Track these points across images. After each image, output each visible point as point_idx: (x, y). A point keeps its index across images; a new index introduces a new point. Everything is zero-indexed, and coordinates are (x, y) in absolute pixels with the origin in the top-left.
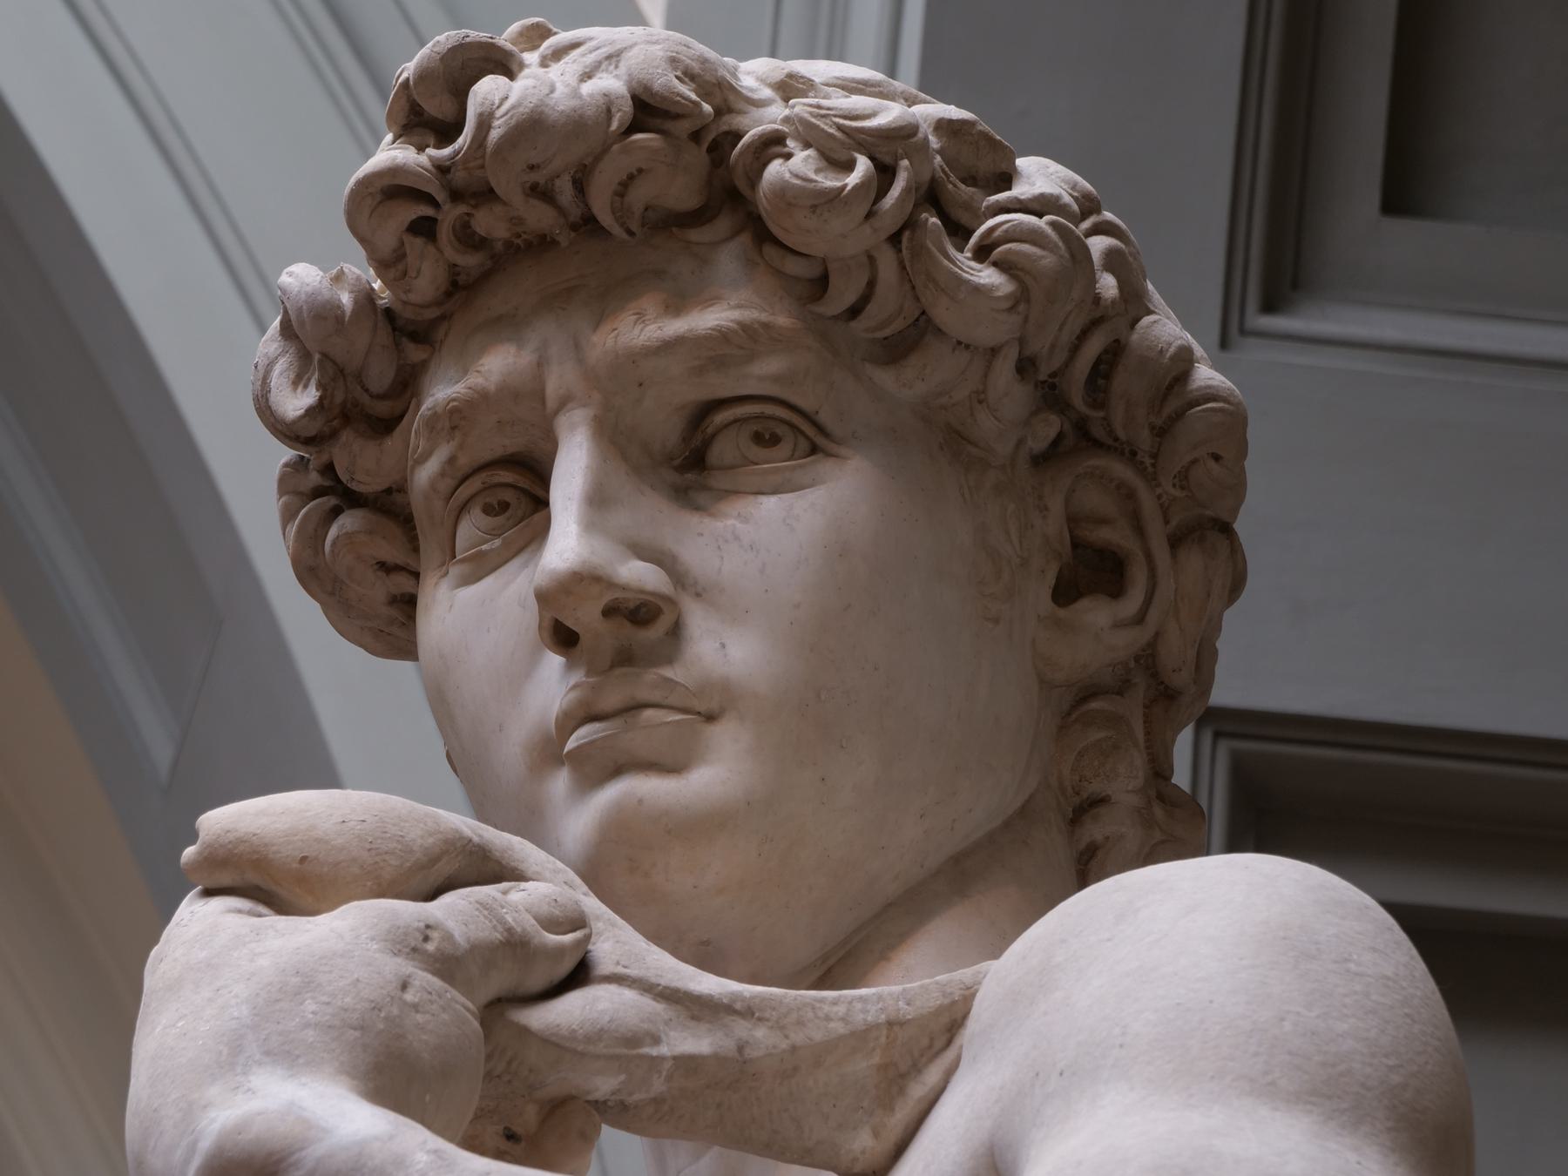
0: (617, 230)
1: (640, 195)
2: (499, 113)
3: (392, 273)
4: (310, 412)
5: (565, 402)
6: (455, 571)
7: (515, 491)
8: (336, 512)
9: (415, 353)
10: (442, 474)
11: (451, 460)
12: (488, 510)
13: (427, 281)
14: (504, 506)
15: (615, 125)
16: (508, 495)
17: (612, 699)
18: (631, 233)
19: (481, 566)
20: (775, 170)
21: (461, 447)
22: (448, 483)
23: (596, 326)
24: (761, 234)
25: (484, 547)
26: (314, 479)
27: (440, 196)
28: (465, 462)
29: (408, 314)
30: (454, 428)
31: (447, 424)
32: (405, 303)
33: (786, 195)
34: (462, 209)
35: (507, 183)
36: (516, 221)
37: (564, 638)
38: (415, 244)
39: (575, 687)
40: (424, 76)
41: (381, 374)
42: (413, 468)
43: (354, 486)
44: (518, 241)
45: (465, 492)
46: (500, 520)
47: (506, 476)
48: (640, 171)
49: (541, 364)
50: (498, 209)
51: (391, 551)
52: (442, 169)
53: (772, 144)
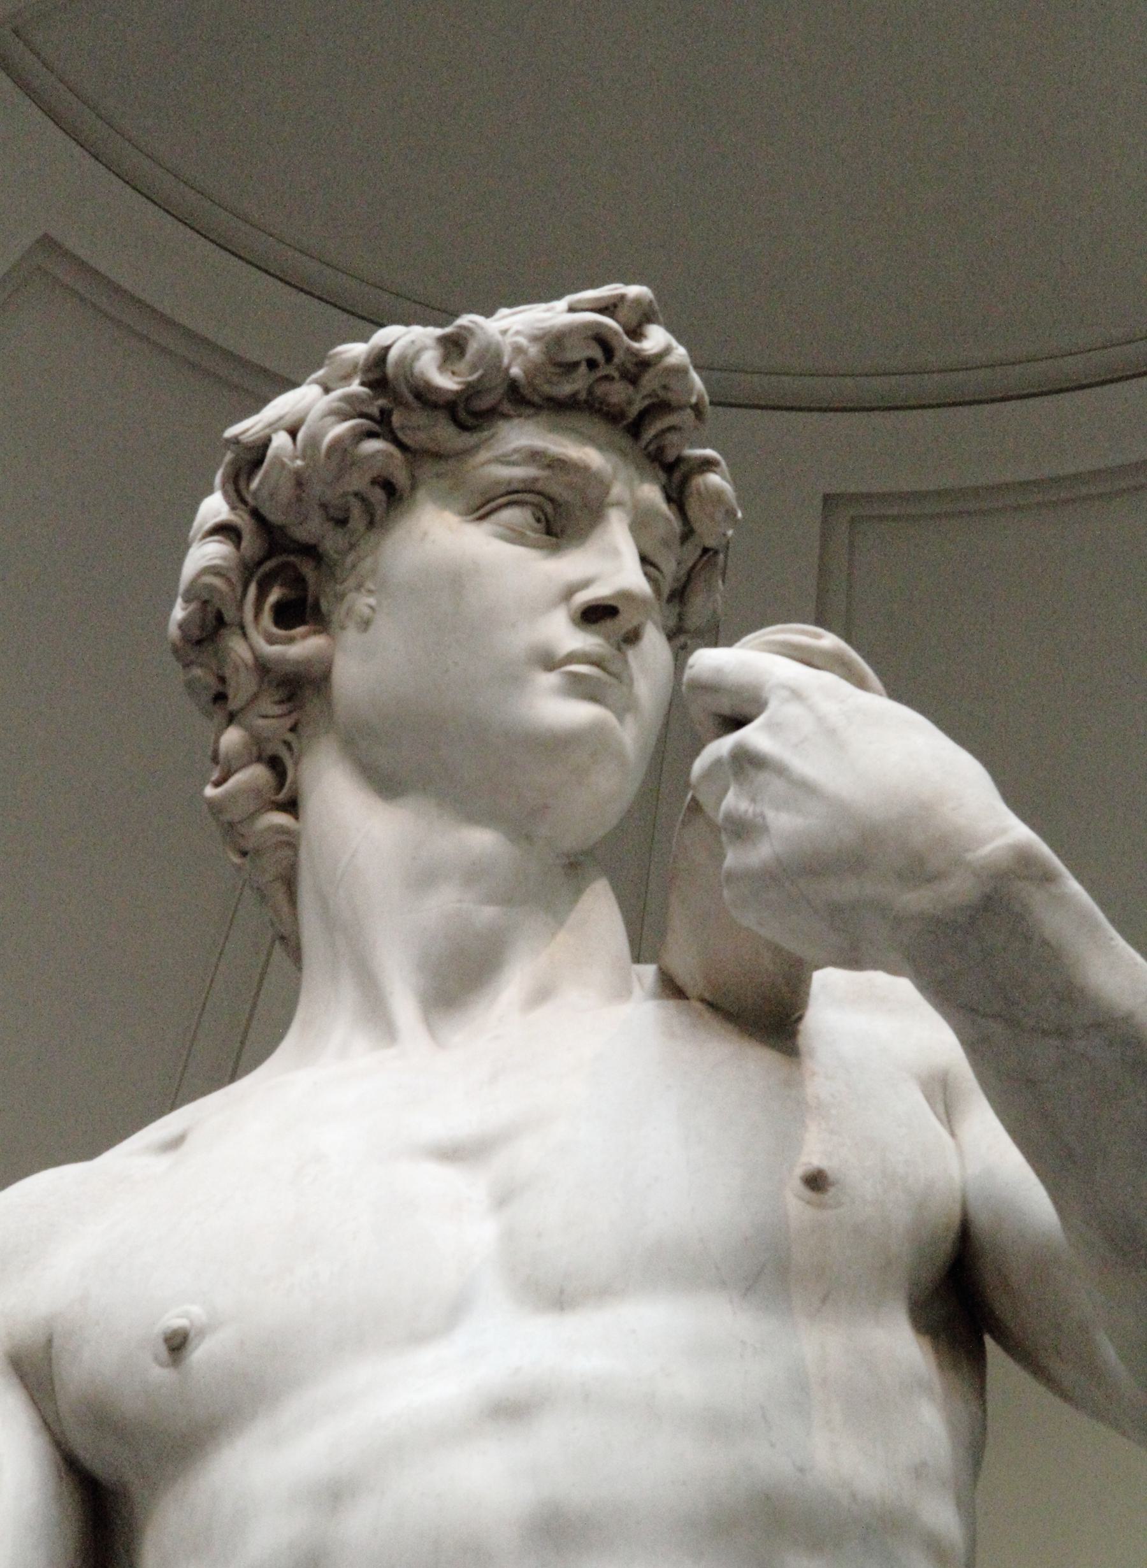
0: (643, 443)
1: (672, 437)
2: (675, 351)
3: (553, 370)
4: (457, 392)
5: (619, 504)
6: (487, 526)
7: (558, 517)
8: (371, 435)
9: (506, 407)
10: (524, 481)
11: (536, 480)
12: (534, 514)
13: (566, 389)
14: (538, 520)
15: (694, 400)
16: (543, 518)
17: (613, 668)
18: (646, 448)
19: (516, 537)
20: (714, 479)
21: (547, 478)
22: (521, 486)
23: (642, 482)
24: (677, 497)
25: (528, 533)
26: (374, 410)
27: (616, 360)
28: (539, 486)
29: (527, 392)
30: (549, 466)
31: (547, 462)
32: (530, 384)
33: (717, 497)
34: (616, 375)
35: (649, 382)
36: (630, 403)
37: (594, 615)
38: (583, 368)
39: (599, 645)
40: (638, 301)
41: (484, 403)
42: (489, 462)
43: (400, 435)
44: (597, 405)
45: (527, 497)
46: (536, 525)
47: (549, 508)
48: (680, 429)
49: (615, 477)
50: (631, 388)
51: (401, 477)
52: (629, 350)
53: (708, 465)
